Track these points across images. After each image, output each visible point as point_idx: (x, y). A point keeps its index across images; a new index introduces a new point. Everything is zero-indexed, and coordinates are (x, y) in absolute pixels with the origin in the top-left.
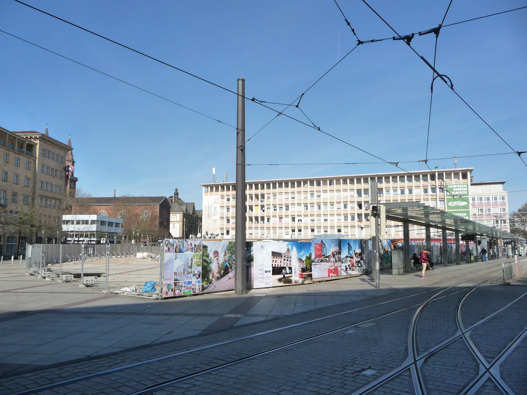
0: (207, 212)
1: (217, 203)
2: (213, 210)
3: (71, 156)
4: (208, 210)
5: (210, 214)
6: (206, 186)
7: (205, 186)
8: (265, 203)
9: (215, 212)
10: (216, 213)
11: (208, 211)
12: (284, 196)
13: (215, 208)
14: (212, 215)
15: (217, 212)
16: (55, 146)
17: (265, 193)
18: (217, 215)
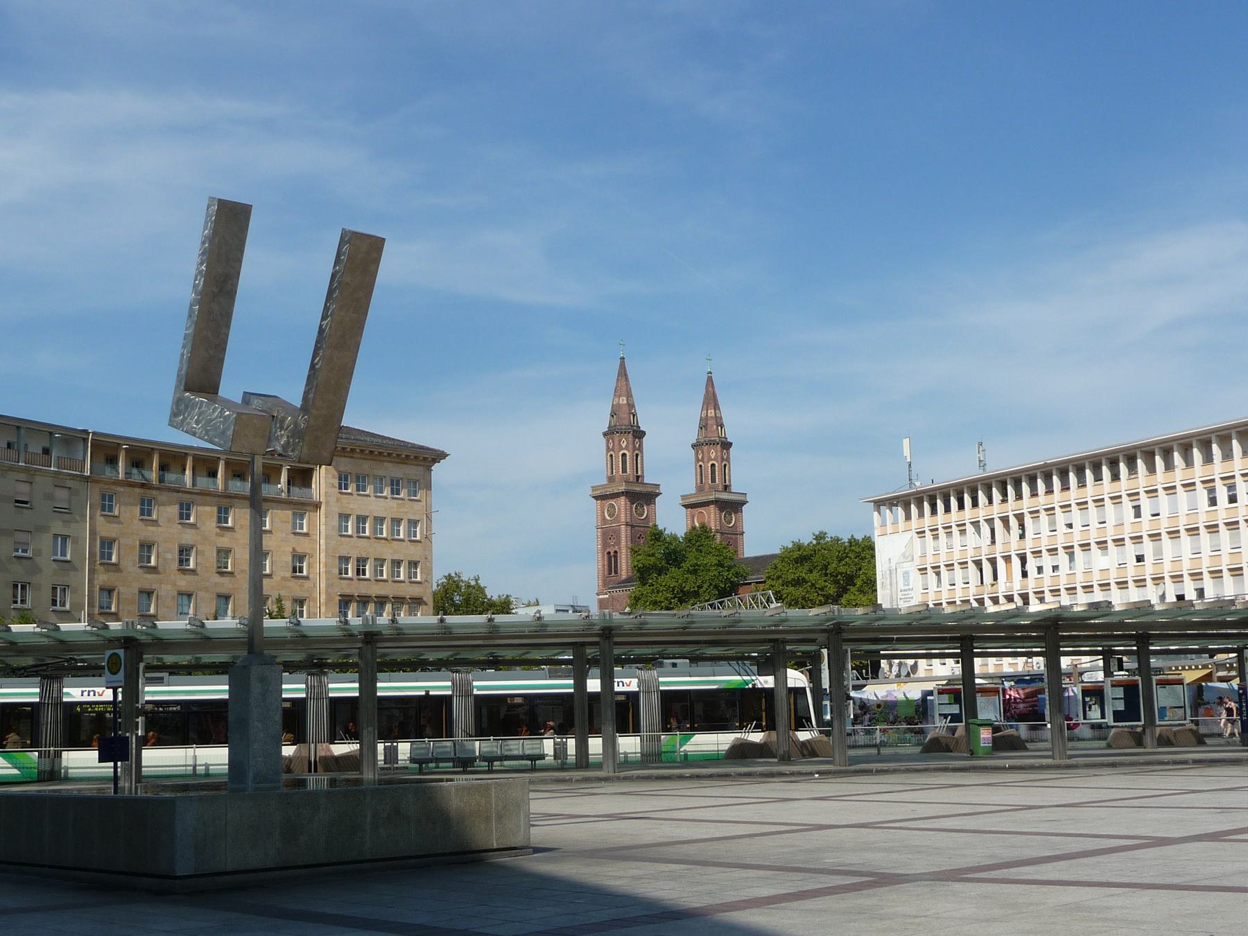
0: (888, 591)
1: (910, 559)
2: (901, 586)
3: (715, 427)
4: (891, 585)
5: (894, 597)
6: (891, 502)
7: (878, 504)
8: (1029, 544)
9: (906, 588)
10: (909, 592)
11: (889, 587)
12: (1076, 516)
13: (906, 574)
14: (900, 599)
15: (910, 587)
16: (383, 458)
17: (1025, 511)
18: (912, 598)
